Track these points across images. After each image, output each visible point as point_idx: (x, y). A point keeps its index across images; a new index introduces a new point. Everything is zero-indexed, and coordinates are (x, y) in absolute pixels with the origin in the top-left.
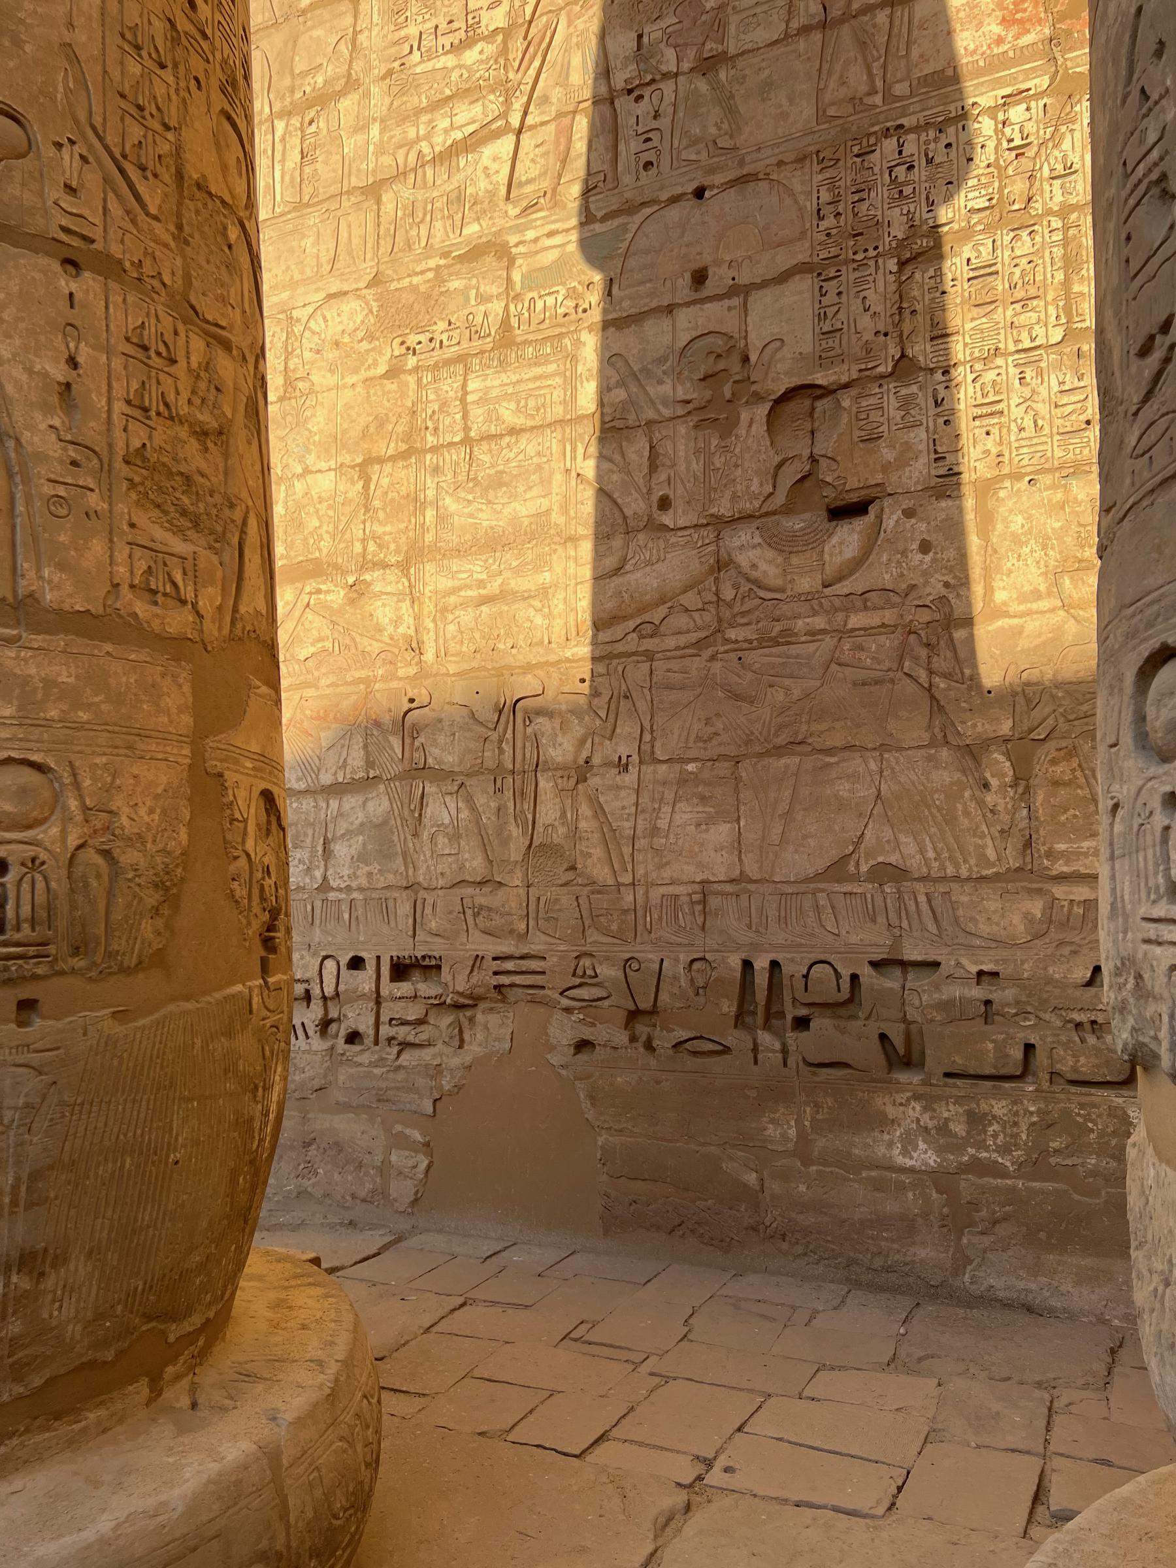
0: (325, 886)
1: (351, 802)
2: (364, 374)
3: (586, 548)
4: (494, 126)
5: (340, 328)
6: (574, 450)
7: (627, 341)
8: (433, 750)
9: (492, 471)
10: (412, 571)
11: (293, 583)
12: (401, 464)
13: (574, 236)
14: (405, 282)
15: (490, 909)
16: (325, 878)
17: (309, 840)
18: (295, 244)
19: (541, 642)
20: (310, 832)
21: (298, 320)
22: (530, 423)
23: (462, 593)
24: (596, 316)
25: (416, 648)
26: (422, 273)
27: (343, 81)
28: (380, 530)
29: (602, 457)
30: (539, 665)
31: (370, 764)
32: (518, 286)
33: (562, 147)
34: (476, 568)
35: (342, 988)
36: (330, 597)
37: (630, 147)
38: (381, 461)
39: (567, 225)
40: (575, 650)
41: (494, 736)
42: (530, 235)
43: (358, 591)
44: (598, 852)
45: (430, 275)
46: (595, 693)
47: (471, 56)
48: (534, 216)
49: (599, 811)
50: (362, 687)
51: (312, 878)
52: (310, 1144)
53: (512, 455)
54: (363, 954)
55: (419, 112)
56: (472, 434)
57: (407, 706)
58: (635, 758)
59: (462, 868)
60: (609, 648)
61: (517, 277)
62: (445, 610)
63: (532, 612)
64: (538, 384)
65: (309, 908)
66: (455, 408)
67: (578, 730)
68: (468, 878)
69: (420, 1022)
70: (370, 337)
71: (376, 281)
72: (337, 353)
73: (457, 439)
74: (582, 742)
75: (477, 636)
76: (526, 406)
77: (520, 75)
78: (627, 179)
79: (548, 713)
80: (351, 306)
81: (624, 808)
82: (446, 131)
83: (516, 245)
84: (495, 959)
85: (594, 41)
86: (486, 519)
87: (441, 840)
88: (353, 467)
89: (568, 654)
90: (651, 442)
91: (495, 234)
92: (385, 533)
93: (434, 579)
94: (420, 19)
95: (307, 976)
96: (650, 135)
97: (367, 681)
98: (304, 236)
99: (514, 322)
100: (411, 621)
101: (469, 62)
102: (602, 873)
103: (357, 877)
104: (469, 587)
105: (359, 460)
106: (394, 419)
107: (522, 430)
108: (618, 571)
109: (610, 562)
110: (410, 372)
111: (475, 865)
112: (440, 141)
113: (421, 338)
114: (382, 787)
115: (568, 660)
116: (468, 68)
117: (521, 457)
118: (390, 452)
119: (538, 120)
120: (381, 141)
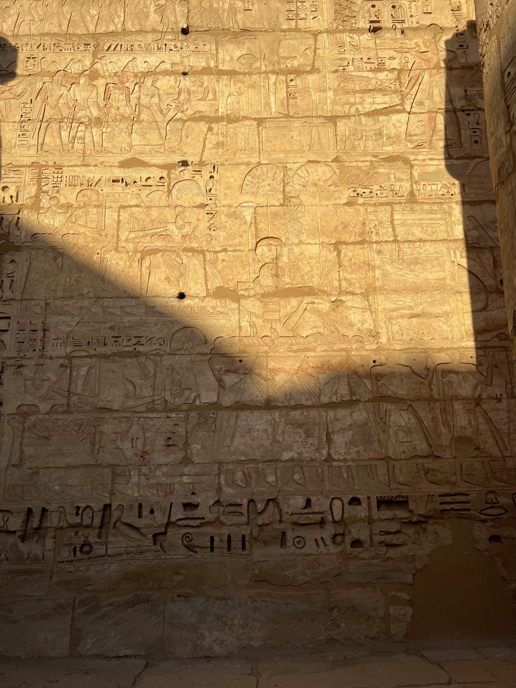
0: (329, 458)
1: (341, 413)
2: (332, 202)
3: (467, 297)
4: (397, 108)
5: (317, 177)
6: (455, 253)
7: (476, 211)
8: (391, 387)
9: (412, 257)
10: (370, 298)
11: (296, 296)
12: (359, 246)
13: (443, 163)
14: (355, 164)
15: (434, 470)
16: (329, 454)
17: (316, 433)
18: (286, 132)
19: (447, 338)
20: (317, 428)
21: (290, 169)
22: (429, 238)
23: (401, 311)
24: (458, 198)
25: (375, 335)
26: (363, 161)
27: (310, 67)
28: (349, 277)
29: (468, 257)
30: (448, 349)
31: (352, 393)
32: (417, 178)
33: (433, 125)
34: (407, 300)
35: (346, 515)
36: (320, 306)
37: (466, 133)
38: (346, 243)
39: (439, 157)
40: (467, 343)
41: (426, 382)
42: (420, 157)
43: (337, 304)
44: (491, 441)
45: (368, 164)
46: (479, 364)
47: (382, 76)
48: (422, 150)
49: (489, 421)
50: (344, 353)
51: (321, 454)
52: (333, 609)
53: (422, 251)
54: (359, 496)
55: (355, 92)
56: (399, 238)
57: (373, 364)
58: (504, 395)
59: (415, 448)
60: (484, 344)
61: (415, 174)
62: (390, 319)
63: (441, 324)
64: (432, 222)
65: (320, 471)
66: (388, 224)
67: (473, 381)
68: (418, 454)
69: (398, 532)
70: (336, 185)
71: (336, 160)
72: (315, 189)
73: (391, 239)
74: (475, 387)
75: (411, 332)
76: (427, 230)
77: (408, 90)
78: (466, 145)
79: (457, 373)
80: (321, 169)
81: (502, 419)
82: (371, 103)
83: (414, 160)
84: (440, 496)
85: (444, 87)
86: (410, 278)
87: (401, 434)
88: (330, 244)
89: (463, 345)
90: (493, 255)
91: (401, 153)
92: (352, 278)
93: (382, 303)
94: (352, 53)
95: (323, 509)
96: (476, 130)
97: (346, 350)
98: (291, 130)
99: (416, 193)
100: (372, 322)
101: (380, 78)
102: (495, 452)
103: (350, 454)
104: (405, 309)
105: (334, 241)
106: (353, 225)
107: (425, 241)
108: (484, 309)
109: (481, 305)
110: (360, 205)
111: (422, 447)
112: (368, 108)
113: (367, 191)
114: (361, 406)
115: (463, 347)
116: (381, 81)
117: (427, 252)
118: (351, 240)
119: (418, 111)
120: (335, 99)
